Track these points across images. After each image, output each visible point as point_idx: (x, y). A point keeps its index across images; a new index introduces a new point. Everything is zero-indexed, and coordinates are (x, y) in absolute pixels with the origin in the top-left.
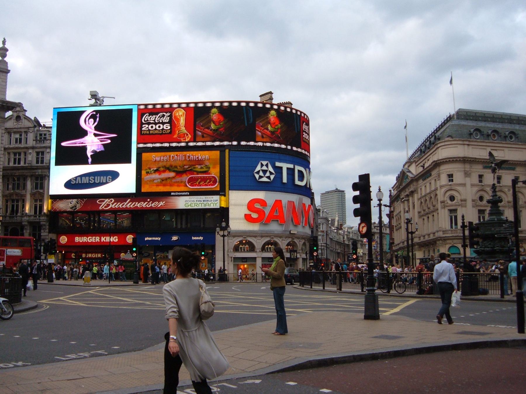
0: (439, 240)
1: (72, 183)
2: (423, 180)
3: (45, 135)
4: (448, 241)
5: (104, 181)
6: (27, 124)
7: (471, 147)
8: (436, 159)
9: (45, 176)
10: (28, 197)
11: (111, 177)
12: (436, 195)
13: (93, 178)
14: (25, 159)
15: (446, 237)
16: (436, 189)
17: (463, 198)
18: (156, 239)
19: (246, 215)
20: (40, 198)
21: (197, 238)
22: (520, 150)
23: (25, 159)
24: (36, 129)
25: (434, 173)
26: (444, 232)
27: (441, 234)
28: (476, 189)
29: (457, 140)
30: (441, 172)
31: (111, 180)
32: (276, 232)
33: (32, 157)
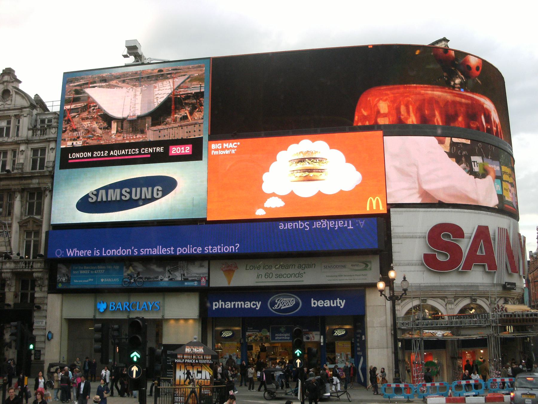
1: (90, 200)
3: (50, 121)
5: (149, 196)
6: (19, 101)
9: (46, 189)
10: (15, 226)
11: (160, 188)
13: (128, 190)
14: (14, 161)
18: (248, 305)
19: (425, 255)
20: (36, 229)
21: (328, 303)
23: (14, 161)
24: (35, 112)
31: (160, 193)
32: (481, 289)
33: (26, 158)
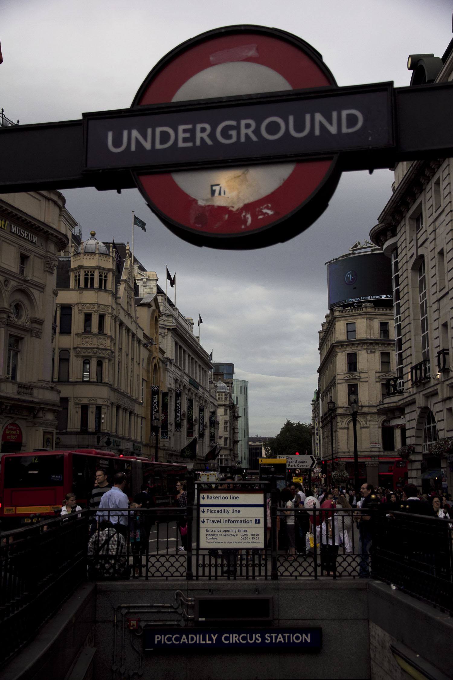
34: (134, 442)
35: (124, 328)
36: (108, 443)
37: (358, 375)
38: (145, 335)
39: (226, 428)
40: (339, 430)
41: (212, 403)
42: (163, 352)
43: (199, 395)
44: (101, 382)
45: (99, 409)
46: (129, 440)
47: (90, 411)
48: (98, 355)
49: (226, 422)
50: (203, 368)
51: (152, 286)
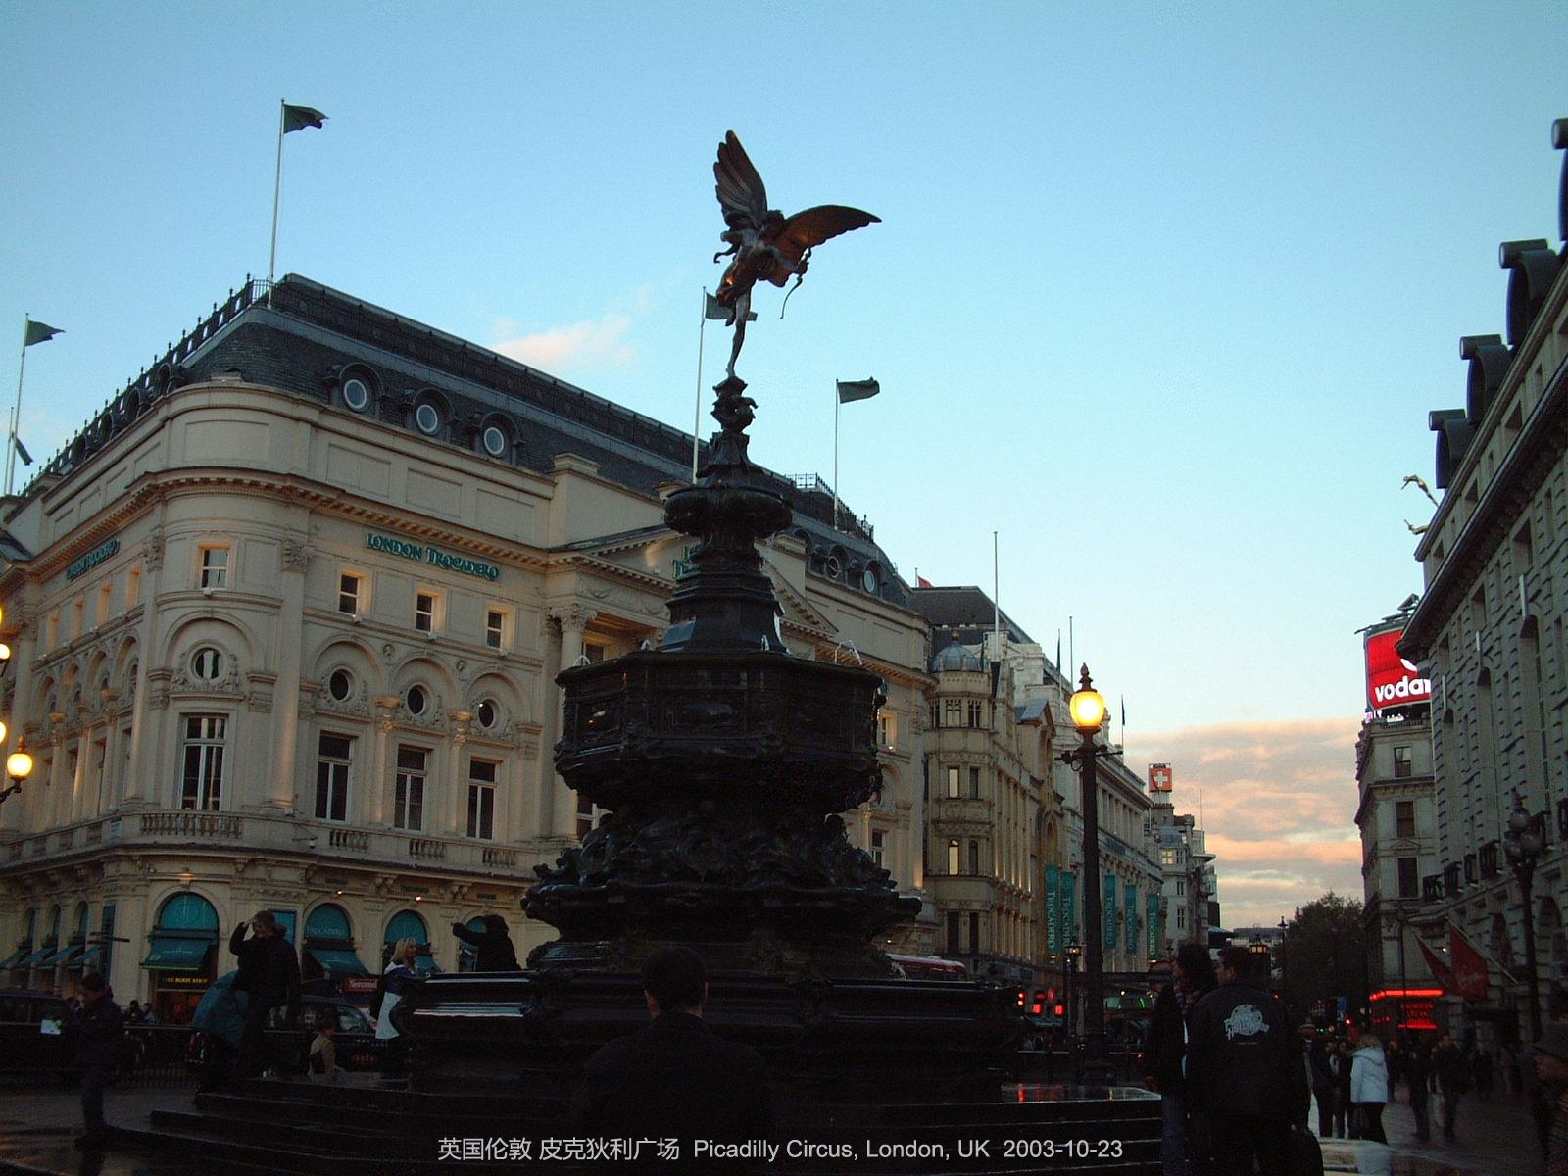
0: (118, 859)
2: (73, 577)
4: (163, 868)
7: (326, 438)
8: (154, 467)
12: (131, 641)
15: (155, 846)
16: (134, 616)
17: (259, 665)
22: (524, 498)
25: (134, 539)
26: (150, 823)
27: (130, 830)
28: (322, 634)
29: (271, 394)
30: (169, 530)
34: (1020, 963)
35: (1003, 779)
36: (993, 971)
37: (1416, 841)
38: (1032, 779)
39: (1180, 923)
40: (1383, 940)
41: (1149, 875)
42: (1060, 798)
43: (1124, 865)
44: (975, 876)
45: (974, 916)
46: (1013, 962)
47: (962, 920)
48: (971, 833)
49: (1180, 910)
50: (1131, 810)
51: (1033, 671)
